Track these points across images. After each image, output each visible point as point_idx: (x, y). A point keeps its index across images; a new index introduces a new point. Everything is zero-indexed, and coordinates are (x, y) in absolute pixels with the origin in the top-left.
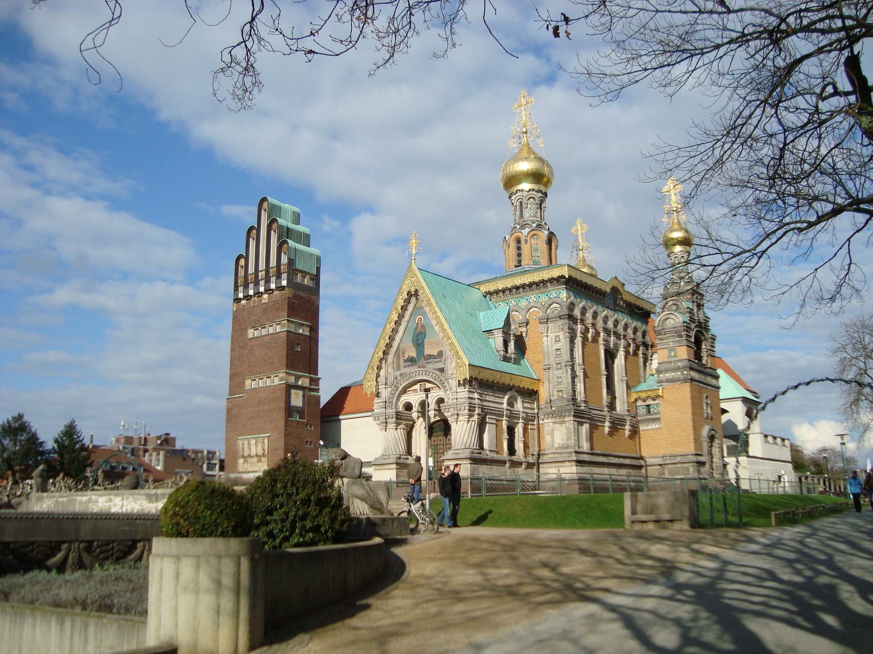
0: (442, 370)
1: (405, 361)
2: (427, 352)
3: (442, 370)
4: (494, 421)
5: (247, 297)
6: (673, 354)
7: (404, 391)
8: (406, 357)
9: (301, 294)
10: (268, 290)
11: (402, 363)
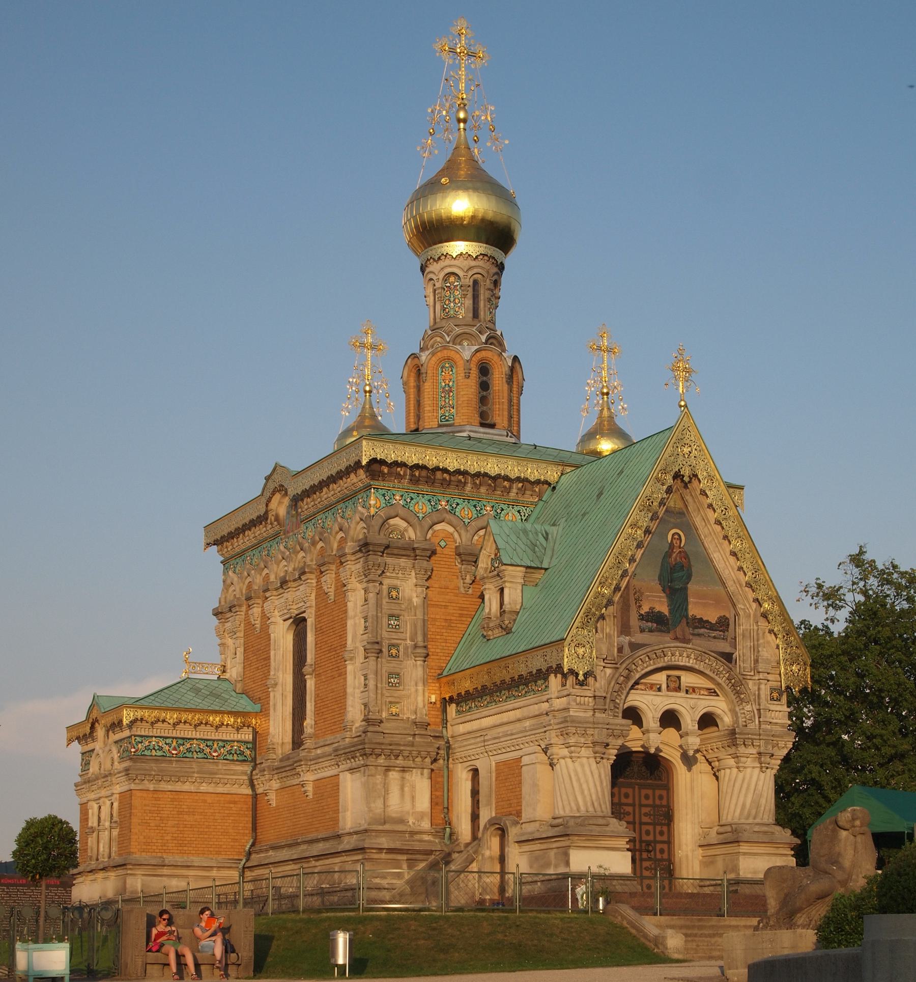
1: (642, 618)
2: (694, 610)
3: (728, 657)
8: (645, 609)
11: (634, 621)
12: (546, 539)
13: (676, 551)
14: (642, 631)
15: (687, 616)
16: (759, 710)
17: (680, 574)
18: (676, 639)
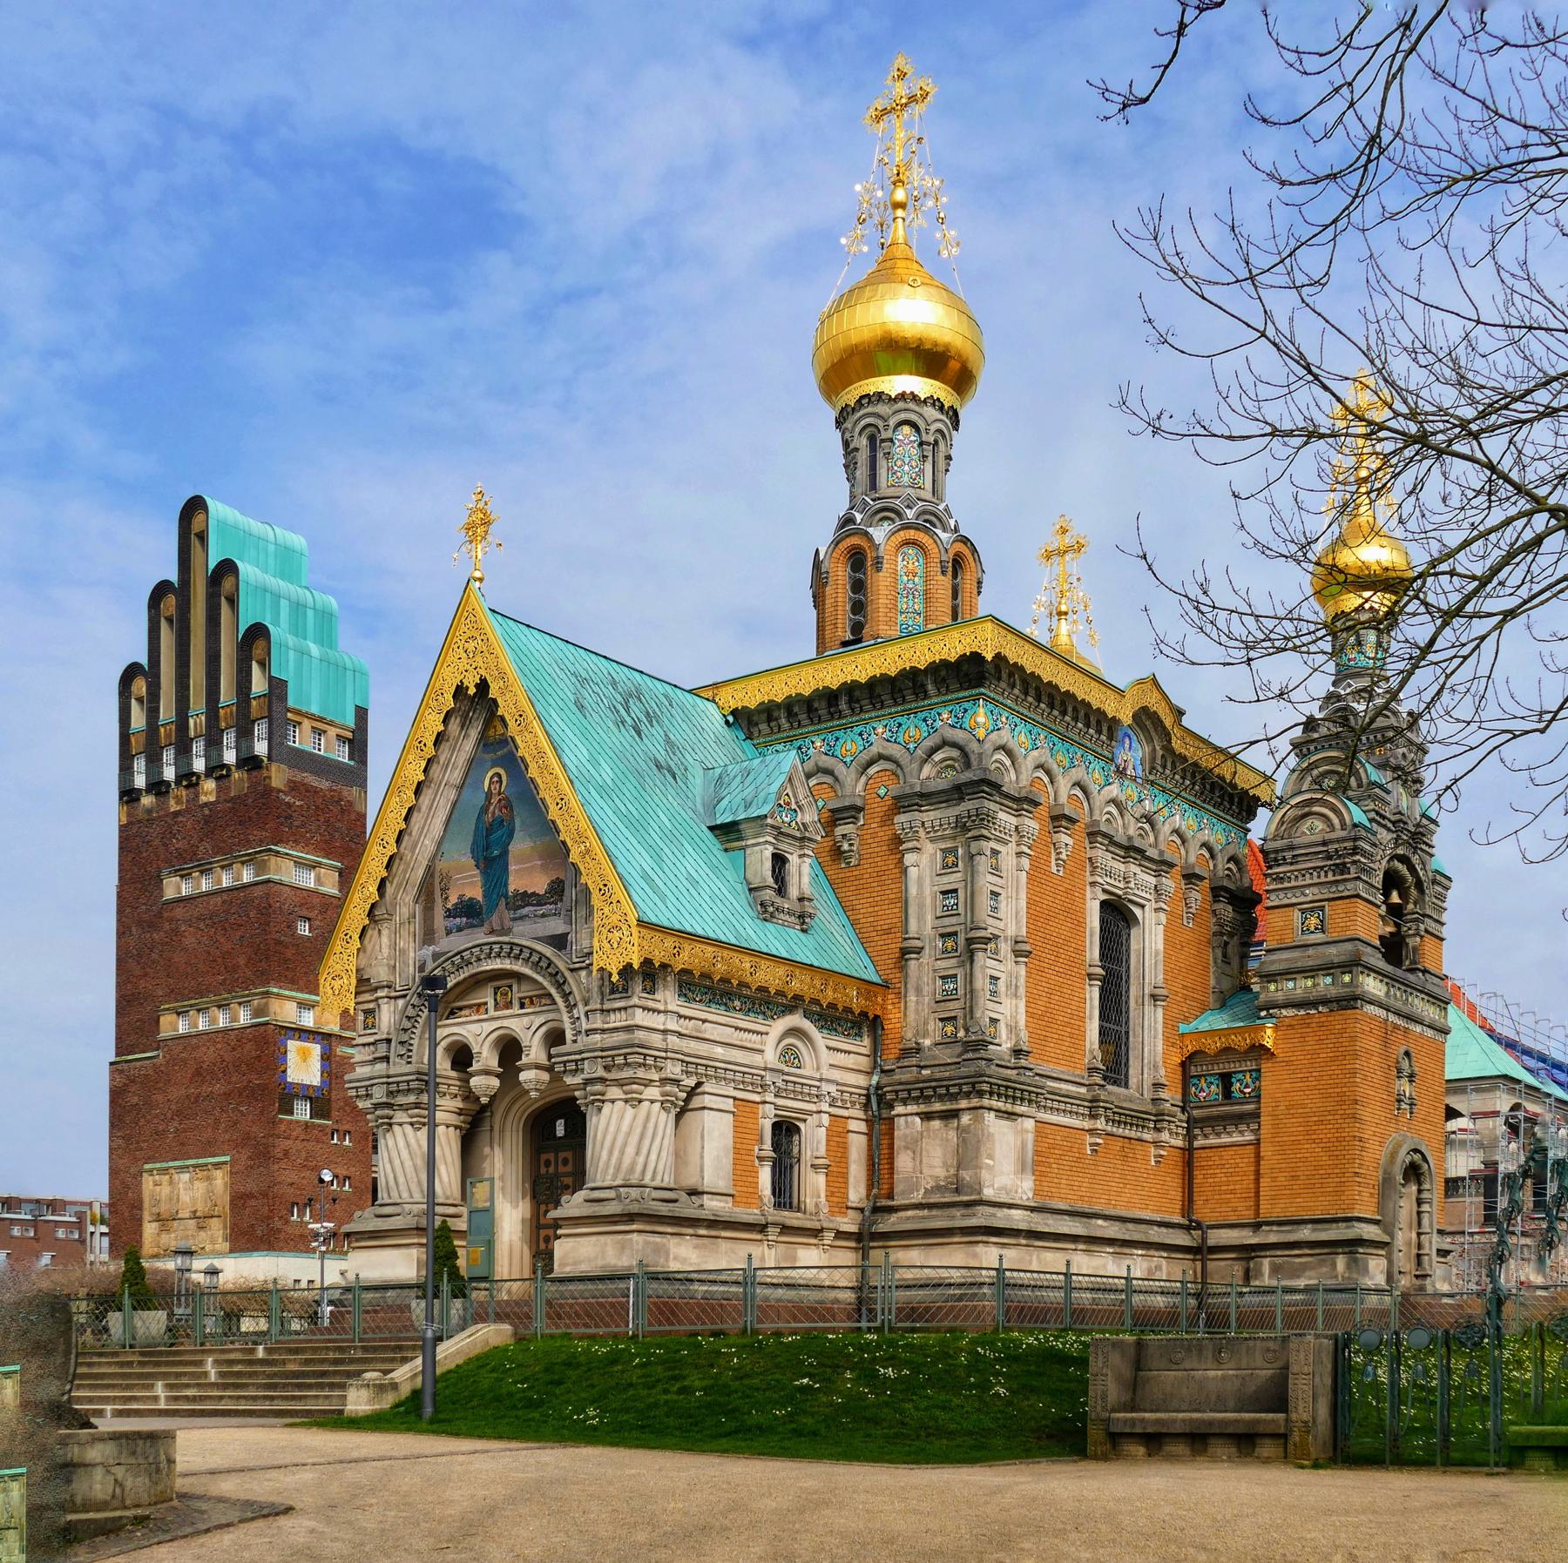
0: (559, 942)
4: (729, 1104)
5: (157, 787)
6: (1313, 921)
9: (311, 780)
10: (216, 770)
15: (506, 897)
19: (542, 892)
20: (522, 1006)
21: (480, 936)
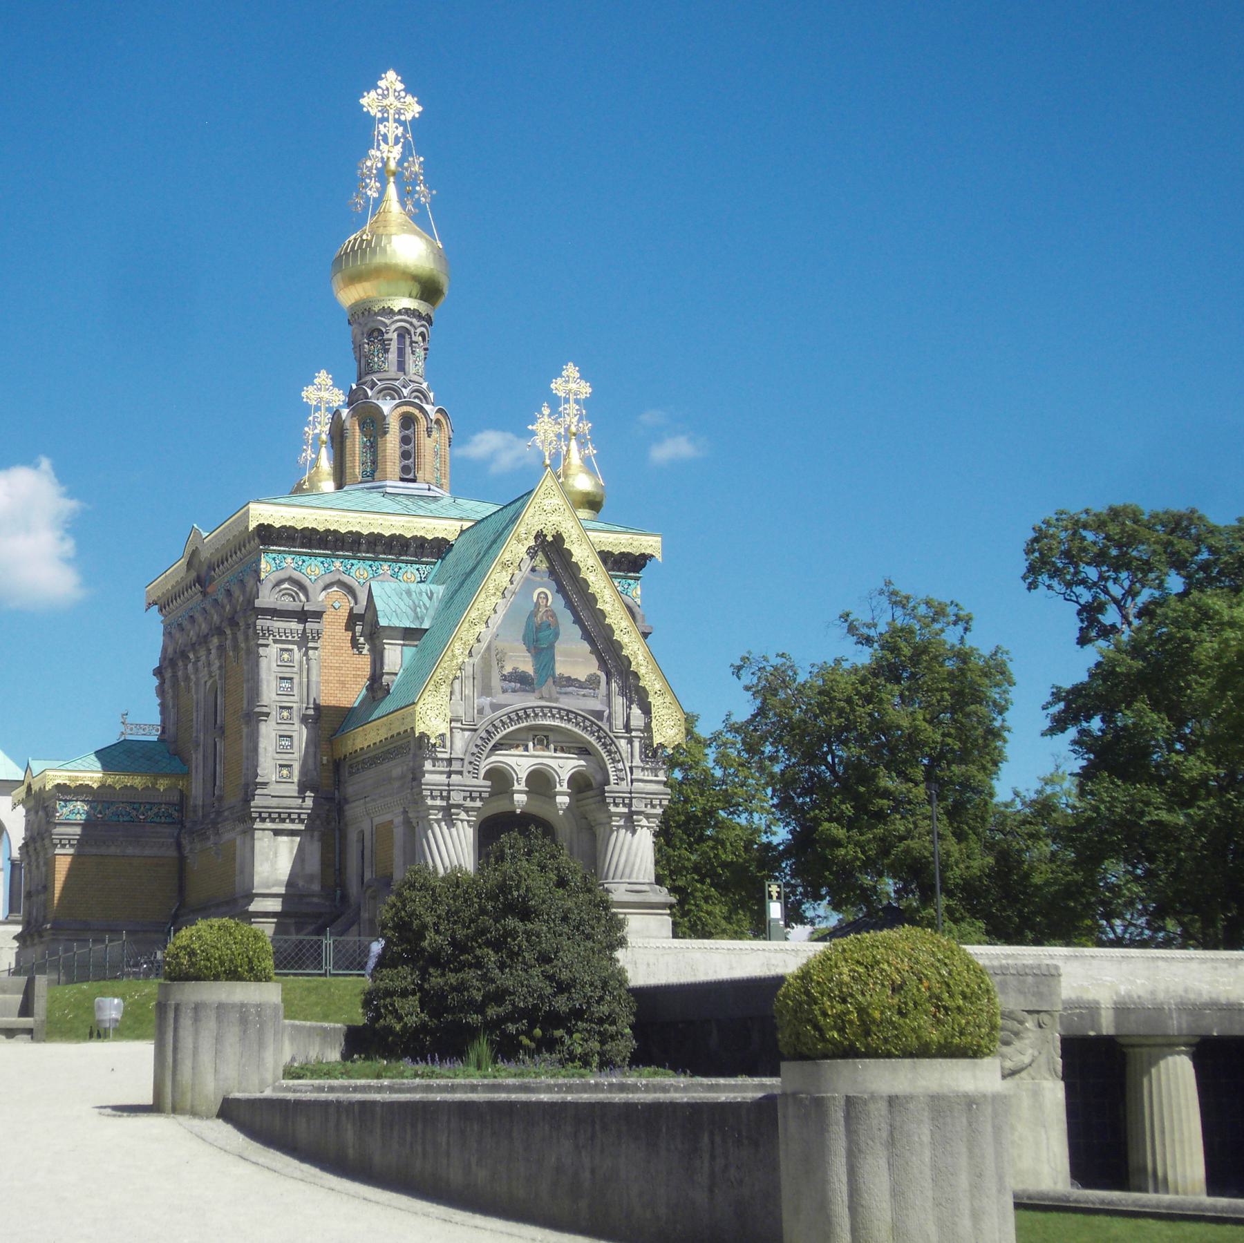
0: (599, 715)
1: (505, 678)
2: (561, 669)
7: (496, 748)
8: (508, 669)
11: (496, 682)
12: (430, 598)
13: (542, 610)
14: (504, 691)
15: (554, 677)
16: (631, 768)
17: (547, 632)
18: (542, 698)
19: (583, 680)
20: (555, 750)
21: (531, 701)
